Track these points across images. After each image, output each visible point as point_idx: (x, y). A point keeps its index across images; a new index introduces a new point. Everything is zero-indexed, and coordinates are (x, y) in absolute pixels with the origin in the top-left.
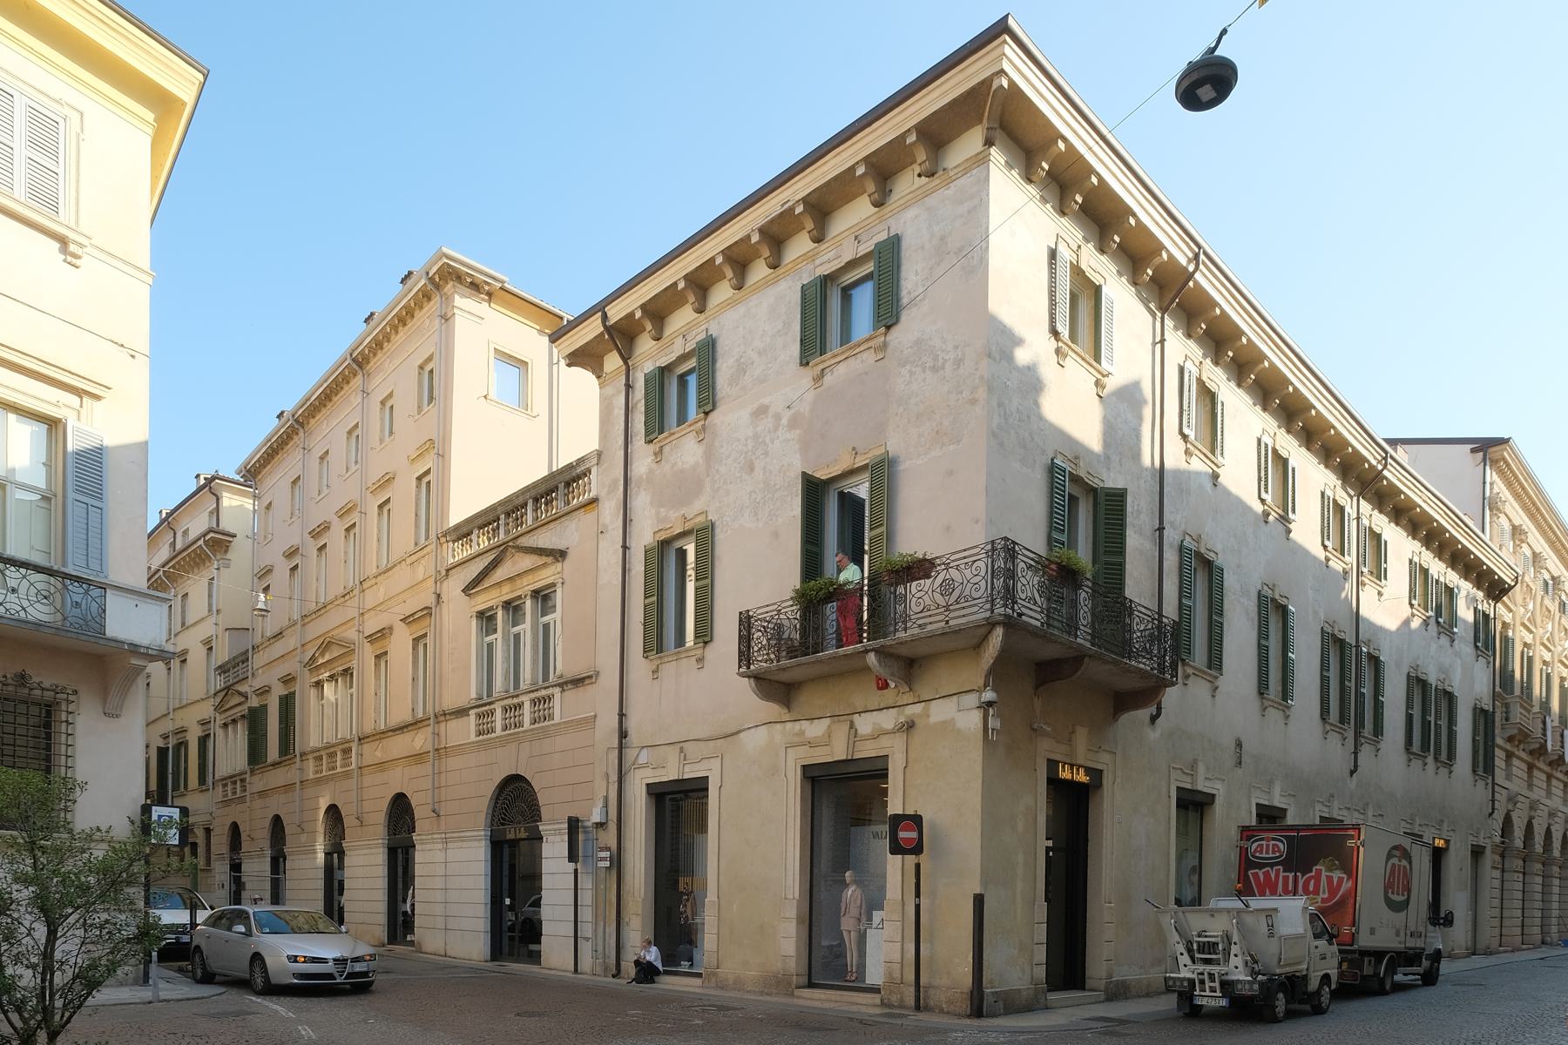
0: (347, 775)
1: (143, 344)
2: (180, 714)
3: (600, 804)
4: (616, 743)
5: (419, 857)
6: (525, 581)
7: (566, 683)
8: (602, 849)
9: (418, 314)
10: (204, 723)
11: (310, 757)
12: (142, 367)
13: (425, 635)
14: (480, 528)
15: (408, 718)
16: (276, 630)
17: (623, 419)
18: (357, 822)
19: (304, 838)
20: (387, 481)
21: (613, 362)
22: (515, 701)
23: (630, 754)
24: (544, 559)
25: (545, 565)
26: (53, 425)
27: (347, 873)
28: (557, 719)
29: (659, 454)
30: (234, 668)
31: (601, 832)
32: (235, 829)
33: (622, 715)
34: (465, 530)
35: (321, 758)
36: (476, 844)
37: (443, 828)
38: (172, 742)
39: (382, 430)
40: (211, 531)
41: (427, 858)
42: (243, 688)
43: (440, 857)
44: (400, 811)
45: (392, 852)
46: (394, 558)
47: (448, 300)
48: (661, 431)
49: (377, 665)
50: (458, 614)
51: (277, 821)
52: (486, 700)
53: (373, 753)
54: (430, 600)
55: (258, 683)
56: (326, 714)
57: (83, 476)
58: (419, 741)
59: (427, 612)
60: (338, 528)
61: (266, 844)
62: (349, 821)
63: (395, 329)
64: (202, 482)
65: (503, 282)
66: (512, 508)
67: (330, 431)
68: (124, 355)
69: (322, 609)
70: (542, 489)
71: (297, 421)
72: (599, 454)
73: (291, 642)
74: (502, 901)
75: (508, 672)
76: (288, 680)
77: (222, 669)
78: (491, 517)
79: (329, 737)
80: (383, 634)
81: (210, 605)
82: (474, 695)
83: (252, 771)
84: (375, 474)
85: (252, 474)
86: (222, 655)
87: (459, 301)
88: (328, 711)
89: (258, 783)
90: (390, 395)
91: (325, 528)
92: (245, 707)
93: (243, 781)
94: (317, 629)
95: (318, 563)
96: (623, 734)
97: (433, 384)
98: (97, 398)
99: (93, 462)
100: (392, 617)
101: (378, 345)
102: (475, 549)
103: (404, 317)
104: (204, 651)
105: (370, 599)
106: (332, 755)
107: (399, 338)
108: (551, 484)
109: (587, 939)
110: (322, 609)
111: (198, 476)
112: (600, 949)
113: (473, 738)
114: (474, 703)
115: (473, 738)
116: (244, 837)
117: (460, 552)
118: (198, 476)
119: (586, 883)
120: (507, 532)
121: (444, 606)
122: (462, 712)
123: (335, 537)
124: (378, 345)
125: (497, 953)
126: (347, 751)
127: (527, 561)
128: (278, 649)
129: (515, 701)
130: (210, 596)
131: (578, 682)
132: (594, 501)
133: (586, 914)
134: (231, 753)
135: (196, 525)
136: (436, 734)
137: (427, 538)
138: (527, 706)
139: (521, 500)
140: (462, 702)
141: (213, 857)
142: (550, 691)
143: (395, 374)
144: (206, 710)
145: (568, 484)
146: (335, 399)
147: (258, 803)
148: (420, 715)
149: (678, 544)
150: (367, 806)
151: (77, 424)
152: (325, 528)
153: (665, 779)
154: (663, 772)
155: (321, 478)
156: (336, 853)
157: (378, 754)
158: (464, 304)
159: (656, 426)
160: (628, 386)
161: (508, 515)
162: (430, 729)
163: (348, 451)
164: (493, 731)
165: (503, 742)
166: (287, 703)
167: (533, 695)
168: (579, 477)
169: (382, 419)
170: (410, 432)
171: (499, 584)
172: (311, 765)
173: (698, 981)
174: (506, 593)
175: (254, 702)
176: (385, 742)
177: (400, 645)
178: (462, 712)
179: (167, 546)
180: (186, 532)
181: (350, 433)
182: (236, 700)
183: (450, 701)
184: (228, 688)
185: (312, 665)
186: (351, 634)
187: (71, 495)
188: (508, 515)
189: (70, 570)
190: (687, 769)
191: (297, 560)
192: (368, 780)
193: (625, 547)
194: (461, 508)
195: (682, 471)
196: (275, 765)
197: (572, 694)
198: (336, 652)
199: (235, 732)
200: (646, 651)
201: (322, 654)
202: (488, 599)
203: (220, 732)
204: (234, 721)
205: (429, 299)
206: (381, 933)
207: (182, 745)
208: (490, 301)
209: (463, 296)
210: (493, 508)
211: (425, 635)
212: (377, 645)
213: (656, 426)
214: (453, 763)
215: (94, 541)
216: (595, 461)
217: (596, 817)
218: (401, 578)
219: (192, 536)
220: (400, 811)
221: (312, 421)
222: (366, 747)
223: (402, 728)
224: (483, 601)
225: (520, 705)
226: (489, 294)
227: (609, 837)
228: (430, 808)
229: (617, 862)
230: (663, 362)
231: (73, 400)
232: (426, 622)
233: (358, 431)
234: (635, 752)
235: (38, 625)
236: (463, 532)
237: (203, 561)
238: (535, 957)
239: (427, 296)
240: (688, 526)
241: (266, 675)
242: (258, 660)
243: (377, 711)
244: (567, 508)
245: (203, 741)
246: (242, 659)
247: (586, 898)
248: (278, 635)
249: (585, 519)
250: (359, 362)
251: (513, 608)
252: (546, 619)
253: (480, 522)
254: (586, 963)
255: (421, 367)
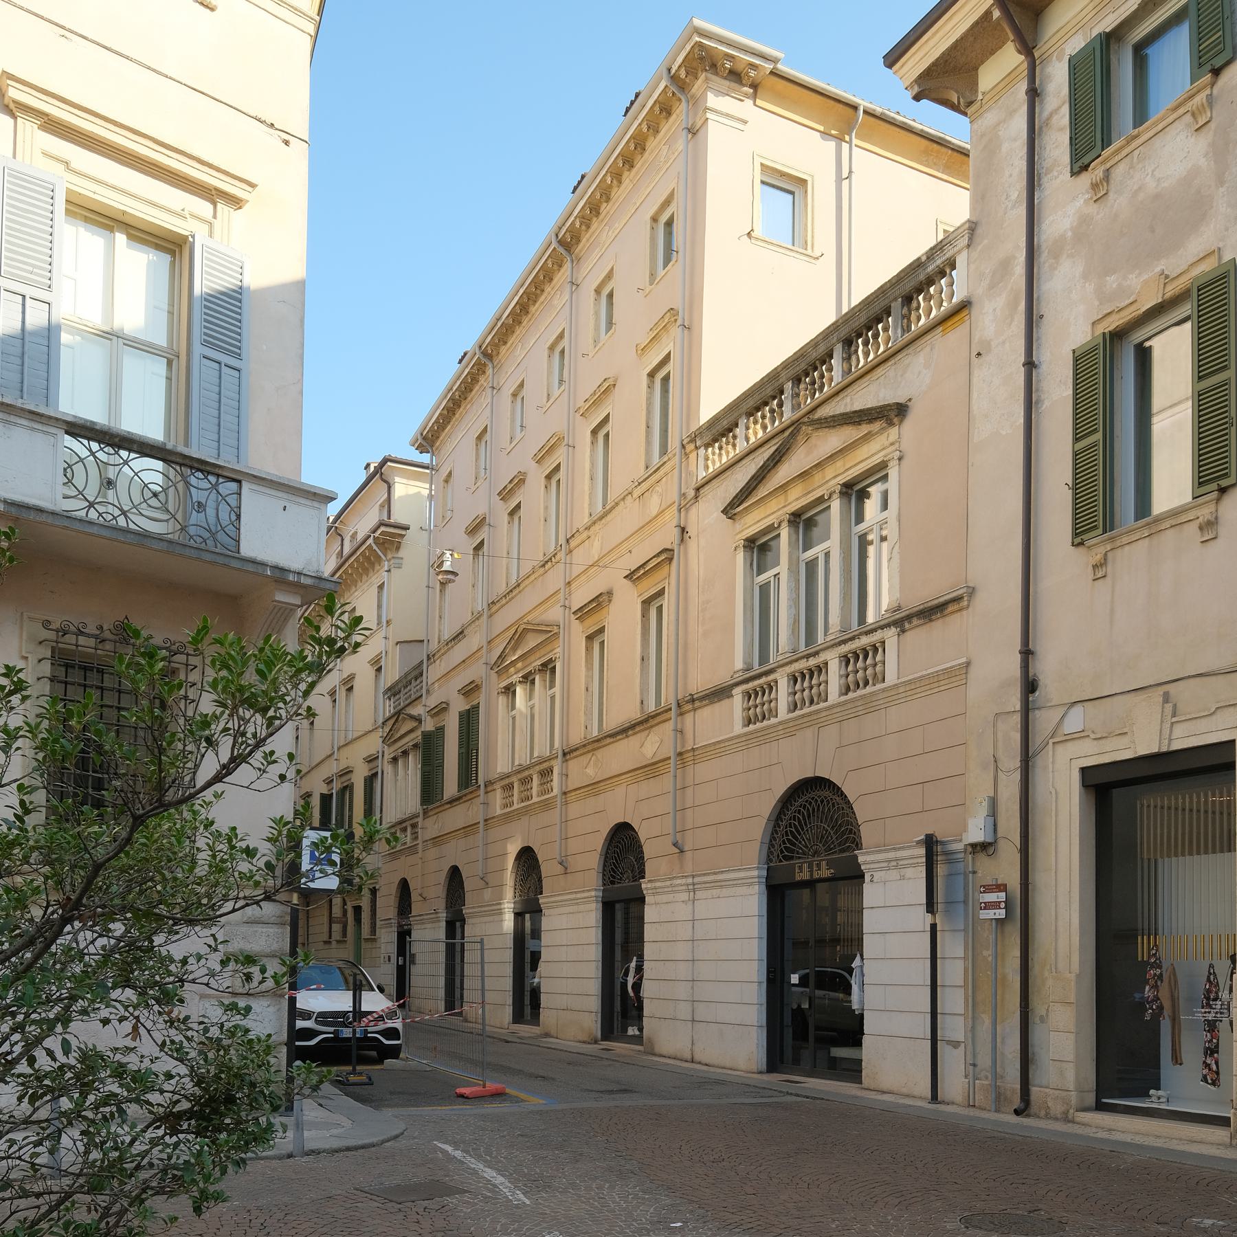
0: (546, 805)
1: (299, 123)
2: (346, 752)
3: (983, 811)
4: (1016, 703)
5: (650, 913)
6: (829, 472)
7: (909, 618)
8: (988, 889)
9: (651, 144)
10: (371, 760)
11: (497, 786)
12: (297, 159)
13: (661, 593)
14: (750, 414)
15: (635, 714)
16: (456, 628)
17: (1023, 152)
18: (560, 869)
19: (487, 894)
20: (606, 390)
21: (1007, 61)
22: (812, 662)
23: (1044, 721)
24: (865, 429)
25: (867, 438)
26: (174, 247)
27: (546, 939)
28: (891, 678)
29: (1100, 191)
30: (406, 688)
31: (982, 858)
32: (404, 886)
33: (1027, 653)
34: (725, 423)
35: (510, 787)
36: (744, 890)
37: (689, 868)
38: (336, 787)
39: (597, 328)
40: (381, 524)
41: (664, 914)
42: (417, 710)
43: (683, 912)
44: (623, 849)
45: (608, 908)
46: (613, 496)
47: (697, 103)
48: (1106, 142)
49: (589, 649)
50: (715, 544)
51: (455, 873)
52: (757, 669)
53: (584, 770)
54: (666, 536)
55: (432, 701)
56: (518, 729)
57: (215, 333)
58: (652, 745)
59: (667, 556)
60: (536, 477)
61: (441, 904)
62: (548, 868)
63: (617, 176)
64: (372, 469)
65: (775, 61)
66: (805, 367)
67: (528, 357)
68: (274, 139)
69: (512, 592)
70: (863, 319)
71: (485, 354)
72: (972, 228)
73: (474, 640)
74: (784, 980)
75: (796, 621)
76: (470, 690)
77: (392, 692)
78: (769, 391)
79: (522, 758)
80: (600, 602)
81: (379, 617)
82: (739, 664)
83: (425, 812)
84: (587, 387)
85: (428, 440)
86: (392, 674)
87: (712, 100)
88: (522, 724)
89: (431, 828)
90: (609, 276)
91: (519, 481)
92: (418, 733)
93: (414, 826)
94: (508, 616)
95: (510, 531)
96: (1030, 686)
97: (673, 237)
98: (236, 202)
99: (230, 305)
100: (613, 577)
101: (594, 209)
102: (741, 446)
103: (628, 157)
104: (371, 672)
105: (581, 557)
106: (526, 781)
107: (618, 194)
108: (877, 308)
109: (956, 1044)
110: (512, 592)
111: (368, 466)
112: (985, 1061)
113: (738, 729)
114: (739, 677)
115: (738, 729)
116: (414, 896)
117: (718, 457)
118: (368, 466)
119: (953, 947)
120: (796, 407)
121: (692, 545)
122: (720, 693)
123: (533, 495)
124: (594, 209)
125: (776, 1060)
126: (546, 773)
127: (833, 440)
128: (460, 652)
129: (812, 662)
130: (379, 606)
131: (931, 612)
132: (965, 306)
133: (953, 1001)
134: (401, 792)
135: (364, 524)
136: (680, 732)
137: (664, 450)
138: (834, 668)
139: (822, 349)
140: (721, 677)
141: (378, 923)
142: (877, 636)
143: (621, 244)
144: (373, 744)
145: (908, 299)
146: (533, 309)
147: (433, 853)
148: (651, 708)
149: (1138, 336)
150: (574, 846)
151: (209, 242)
152: (519, 481)
153: (1128, 755)
154: (1124, 741)
155: (513, 421)
156: (530, 909)
157: (590, 771)
158: (721, 104)
159: (1092, 138)
160: (1034, 94)
161: (797, 380)
162: (669, 726)
163: (550, 373)
164: (773, 713)
165: (790, 729)
166: (469, 720)
167: (844, 649)
168: (930, 281)
169: (597, 313)
170: (637, 316)
171: (784, 488)
172: (498, 797)
173: (1220, 1134)
174: (796, 499)
175: (429, 725)
176: (599, 753)
177: (624, 615)
178: (720, 693)
179: (334, 557)
180: (354, 536)
181: (552, 348)
182: (410, 725)
183: (699, 682)
184: (398, 714)
185: (500, 666)
186: (555, 614)
187: (198, 349)
188: (797, 380)
189: (194, 452)
190: (1179, 731)
191: (483, 534)
192: (575, 809)
193: (1030, 365)
194: (716, 393)
195: (1157, 197)
196: (453, 801)
197: (918, 636)
198: (532, 641)
199: (406, 767)
200: (1080, 534)
201: (514, 649)
202: (767, 514)
203: (388, 769)
204: (405, 753)
205: (669, 114)
206: (592, 1022)
207: (347, 789)
208: (754, 97)
209: (720, 93)
210: (774, 376)
211: (661, 593)
212: (589, 621)
213: (1092, 138)
214: (702, 771)
215: (228, 419)
216: (965, 241)
217: (976, 832)
218: (627, 518)
219: (360, 537)
220: (623, 849)
221: (503, 349)
222: (574, 765)
223: (625, 731)
224: (753, 522)
225: (822, 669)
226: (755, 86)
227: (1006, 868)
228: (669, 841)
229: (1022, 912)
230: (1108, 23)
231: (203, 207)
232: (664, 571)
233: (565, 343)
234: (1056, 715)
235: (145, 535)
236: (722, 429)
237: (372, 565)
238: (853, 1071)
239: (665, 109)
240: (1172, 290)
241: (442, 690)
242: (433, 673)
243: (588, 712)
244: (908, 337)
245: (370, 781)
246: (415, 674)
247: (953, 972)
248: (459, 636)
249: (950, 342)
250: (567, 243)
251: (805, 522)
252: (862, 527)
253: (751, 403)
254: (954, 1083)
255: (655, 219)
